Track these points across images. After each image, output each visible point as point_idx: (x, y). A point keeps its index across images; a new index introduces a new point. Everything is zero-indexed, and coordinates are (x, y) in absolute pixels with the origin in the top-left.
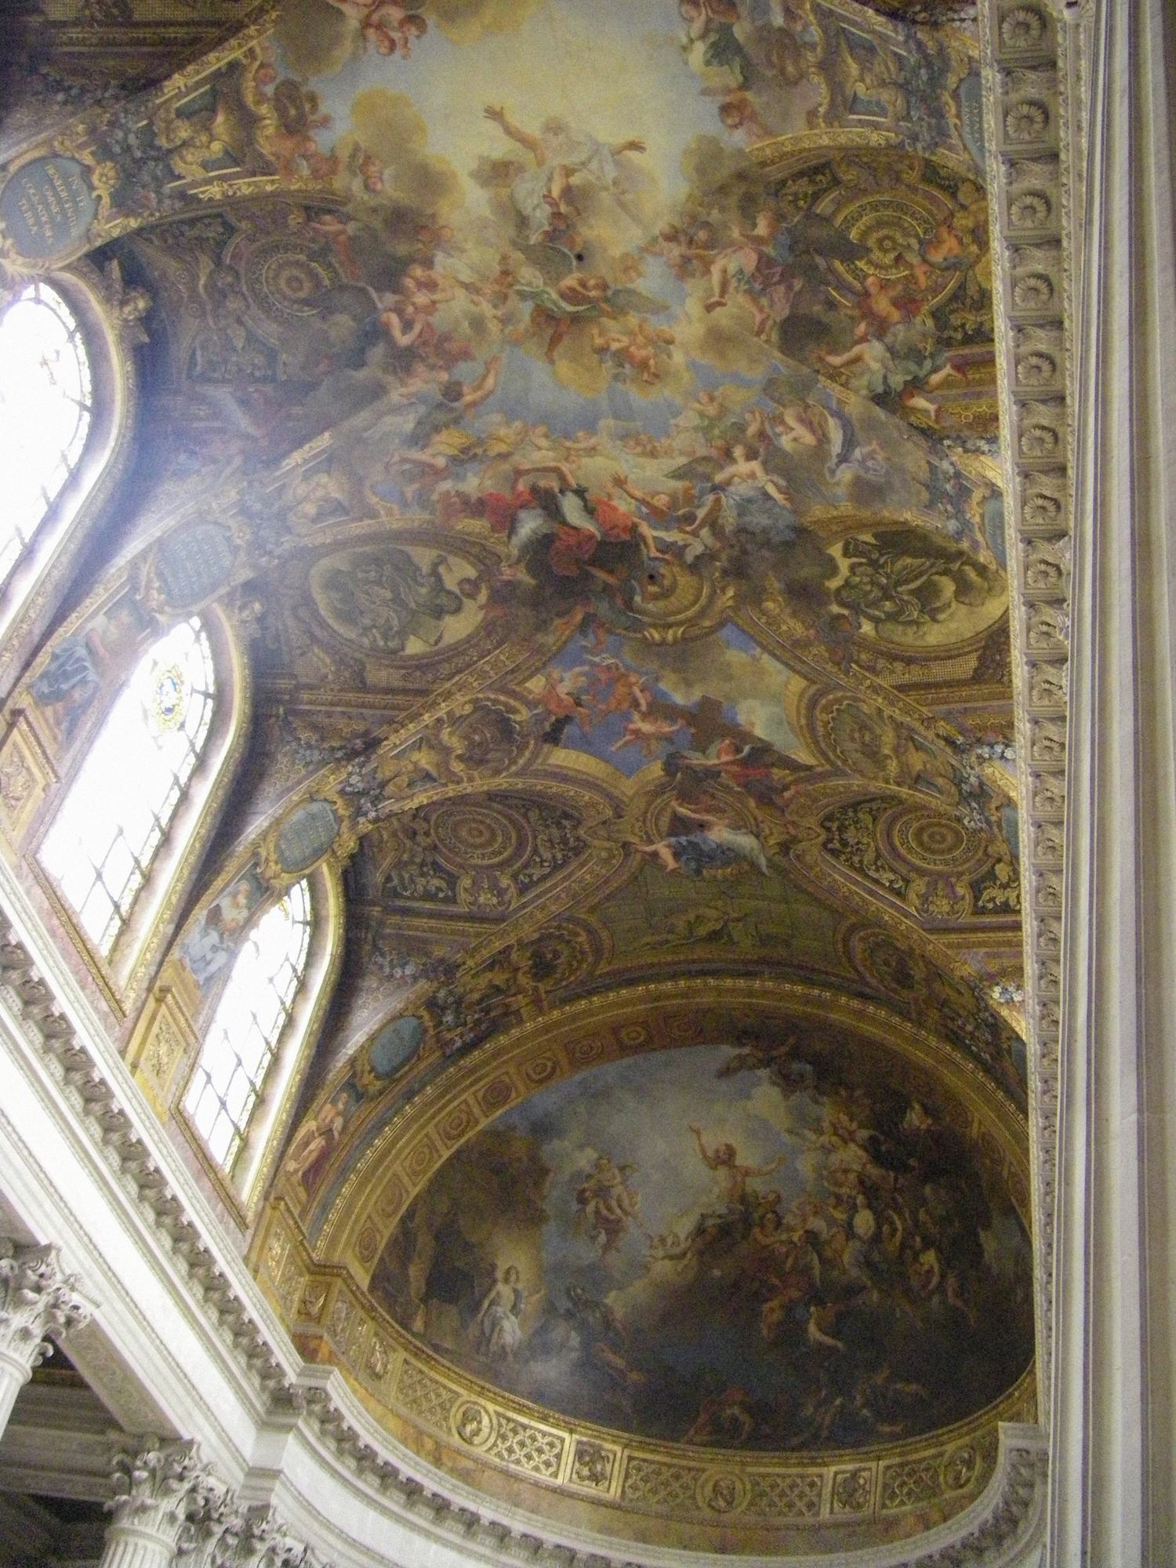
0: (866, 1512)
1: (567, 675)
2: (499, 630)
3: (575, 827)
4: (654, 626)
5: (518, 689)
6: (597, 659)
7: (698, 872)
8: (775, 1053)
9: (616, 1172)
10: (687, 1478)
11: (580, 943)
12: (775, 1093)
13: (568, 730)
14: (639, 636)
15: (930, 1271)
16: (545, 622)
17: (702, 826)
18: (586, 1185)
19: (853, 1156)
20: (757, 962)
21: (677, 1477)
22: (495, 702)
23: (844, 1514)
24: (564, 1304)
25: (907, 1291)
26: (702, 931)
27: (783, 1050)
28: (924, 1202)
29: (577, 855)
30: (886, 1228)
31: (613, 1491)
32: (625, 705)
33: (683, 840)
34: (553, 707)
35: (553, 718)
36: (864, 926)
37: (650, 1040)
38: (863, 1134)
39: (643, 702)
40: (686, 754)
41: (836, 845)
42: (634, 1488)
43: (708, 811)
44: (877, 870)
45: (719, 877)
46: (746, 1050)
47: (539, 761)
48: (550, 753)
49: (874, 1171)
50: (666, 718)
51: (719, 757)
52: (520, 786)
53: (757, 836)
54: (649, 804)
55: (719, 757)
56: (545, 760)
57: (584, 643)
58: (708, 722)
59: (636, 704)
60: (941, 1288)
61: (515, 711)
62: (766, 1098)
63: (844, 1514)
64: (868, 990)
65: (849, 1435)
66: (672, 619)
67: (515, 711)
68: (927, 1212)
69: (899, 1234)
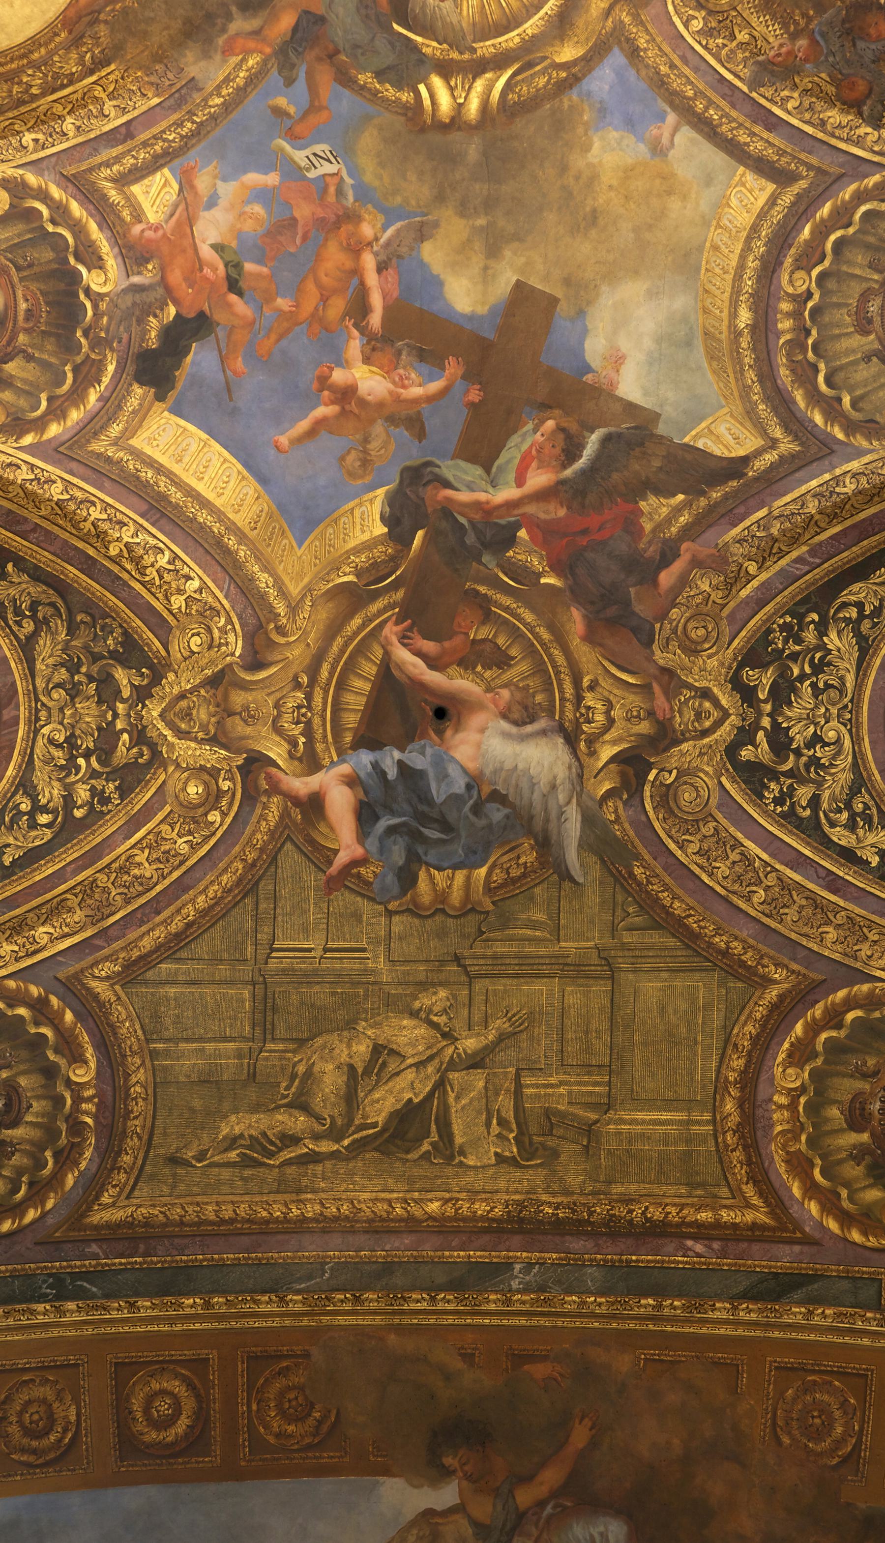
1: (227, 190)
2: (102, 30)
3: (142, 694)
4: (446, 70)
5: (114, 195)
6: (300, 156)
7: (407, 878)
11: (76, 1088)
13: (199, 359)
14: (406, 97)
16: (209, 17)
17: (444, 713)
20: (496, 1230)
22: (60, 213)
29: (124, 792)
32: (337, 307)
33: (390, 759)
34: (176, 277)
35: (172, 310)
39: (376, 301)
40: (449, 469)
43: (466, 664)
44: (851, 826)
45: (456, 897)
47: (115, 429)
48: (141, 415)
50: (422, 355)
51: (520, 482)
52: (56, 492)
53: (571, 741)
54: (333, 630)
55: (520, 482)
56: (130, 431)
57: (282, 102)
58: (514, 368)
59: (359, 308)
61: (96, 262)
64: (786, 1259)
66: (487, 48)
67: (96, 262)
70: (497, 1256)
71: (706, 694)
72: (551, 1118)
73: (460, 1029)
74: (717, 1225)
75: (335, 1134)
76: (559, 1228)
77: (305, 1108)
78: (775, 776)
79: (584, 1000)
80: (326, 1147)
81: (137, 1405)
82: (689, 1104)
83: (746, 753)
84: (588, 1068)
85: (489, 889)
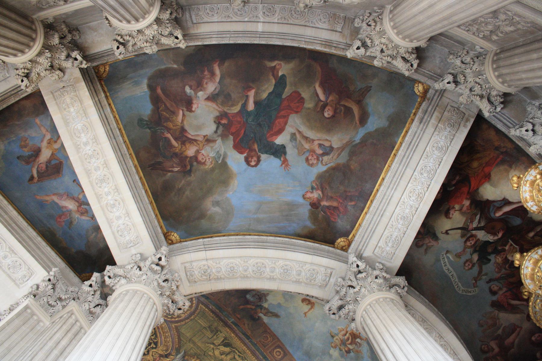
8: (254, 307)
9: (335, 339)
18: (344, 350)
20: (229, 327)
26: (227, 349)
27: (249, 306)
36: (172, 322)
37: (279, 347)
41: (153, 345)
46: (261, 315)
70: (232, 324)
71: (152, 356)
72: (212, 332)
73: (211, 348)
74: (206, 308)
75: (234, 352)
76: (222, 321)
77: (234, 357)
78: (154, 342)
79: (196, 339)
80: (236, 351)
81: (280, 357)
82: (196, 321)
83: (154, 346)
84: (203, 333)
85: (194, 358)
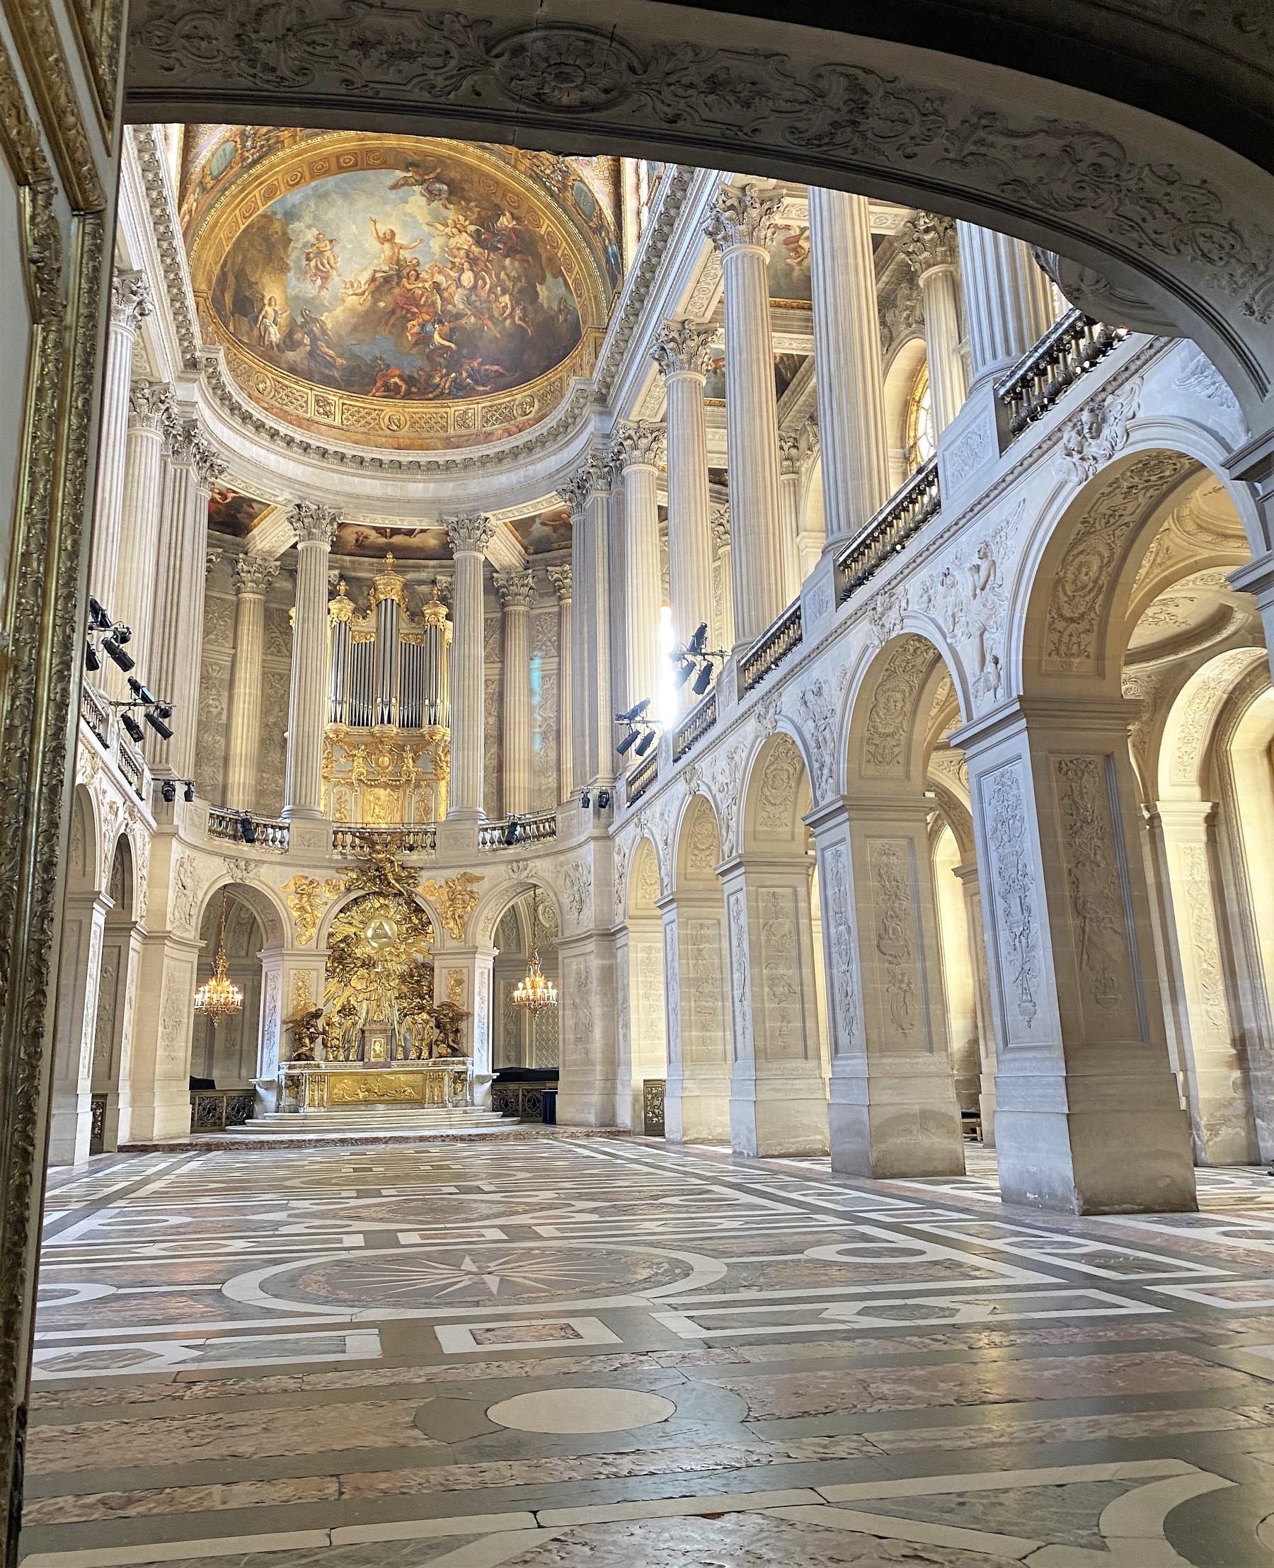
0: (472, 430)
10: (374, 414)
12: (422, 201)
15: (506, 306)
19: (464, 241)
21: (368, 414)
23: (464, 431)
24: (300, 320)
25: (491, 317)
28: (504, 268)
30: (480, 283)
31: (337, 422)
38: (472, 228)
42: (348, 420)
49: (476, 249)
60: (511, 315)
62: (416, 202)
63: (464, 431)
65: (460, 391)
68: (507, 275)
69: (488, 286)
